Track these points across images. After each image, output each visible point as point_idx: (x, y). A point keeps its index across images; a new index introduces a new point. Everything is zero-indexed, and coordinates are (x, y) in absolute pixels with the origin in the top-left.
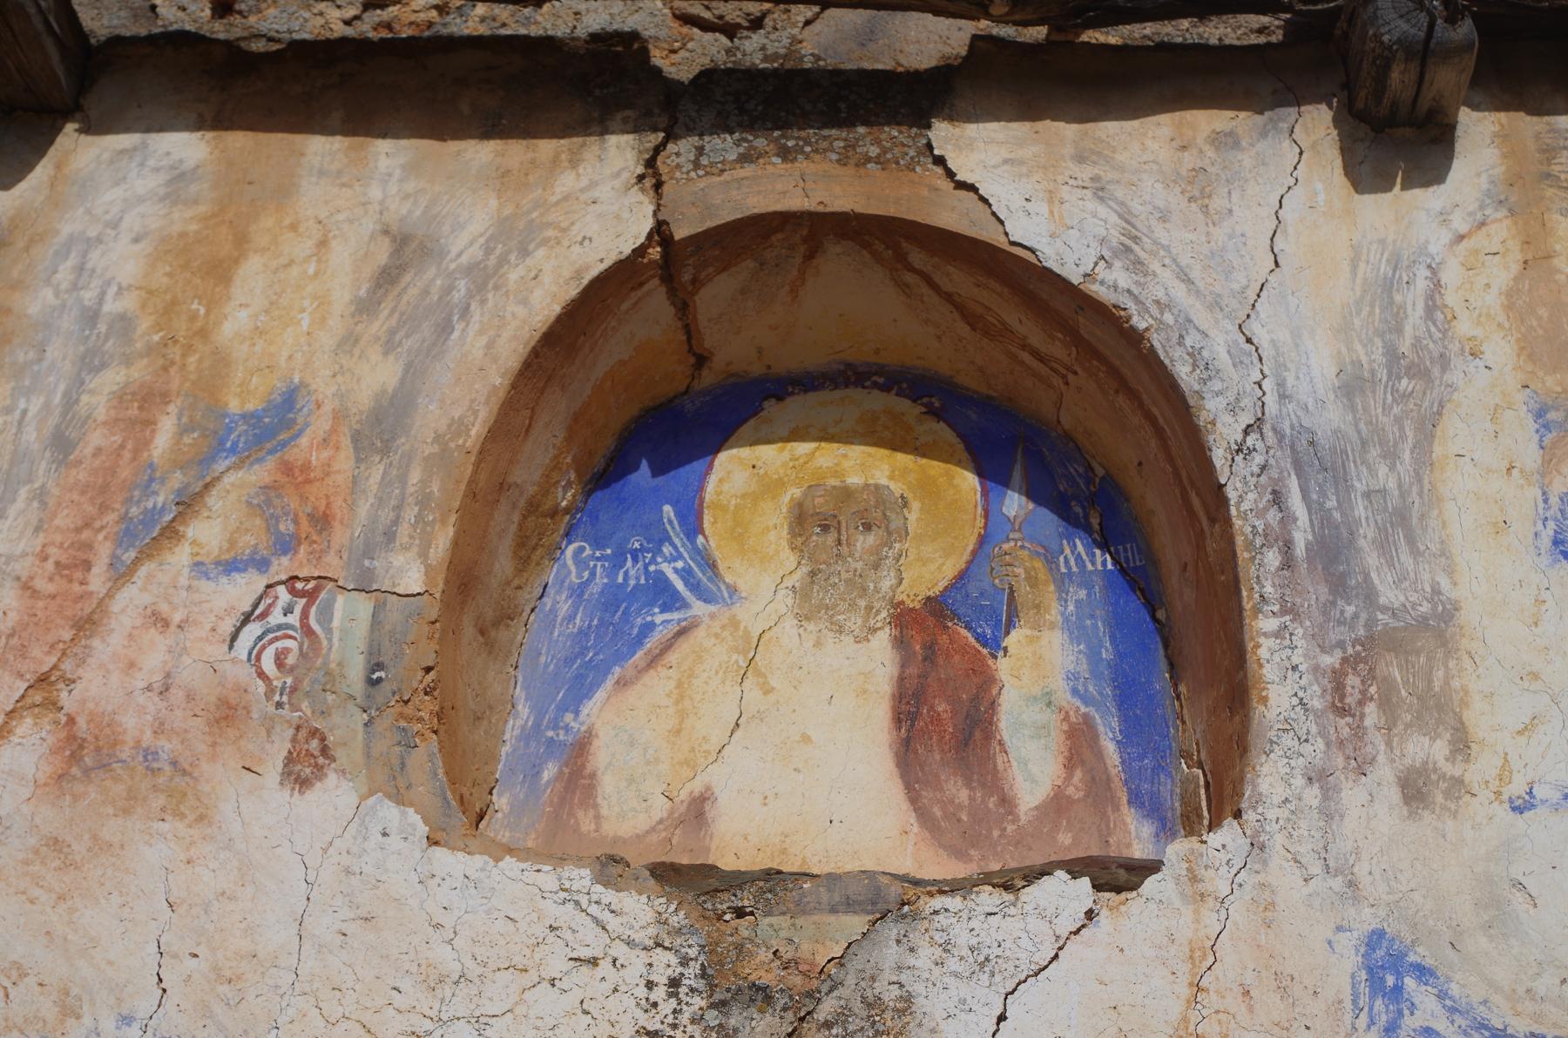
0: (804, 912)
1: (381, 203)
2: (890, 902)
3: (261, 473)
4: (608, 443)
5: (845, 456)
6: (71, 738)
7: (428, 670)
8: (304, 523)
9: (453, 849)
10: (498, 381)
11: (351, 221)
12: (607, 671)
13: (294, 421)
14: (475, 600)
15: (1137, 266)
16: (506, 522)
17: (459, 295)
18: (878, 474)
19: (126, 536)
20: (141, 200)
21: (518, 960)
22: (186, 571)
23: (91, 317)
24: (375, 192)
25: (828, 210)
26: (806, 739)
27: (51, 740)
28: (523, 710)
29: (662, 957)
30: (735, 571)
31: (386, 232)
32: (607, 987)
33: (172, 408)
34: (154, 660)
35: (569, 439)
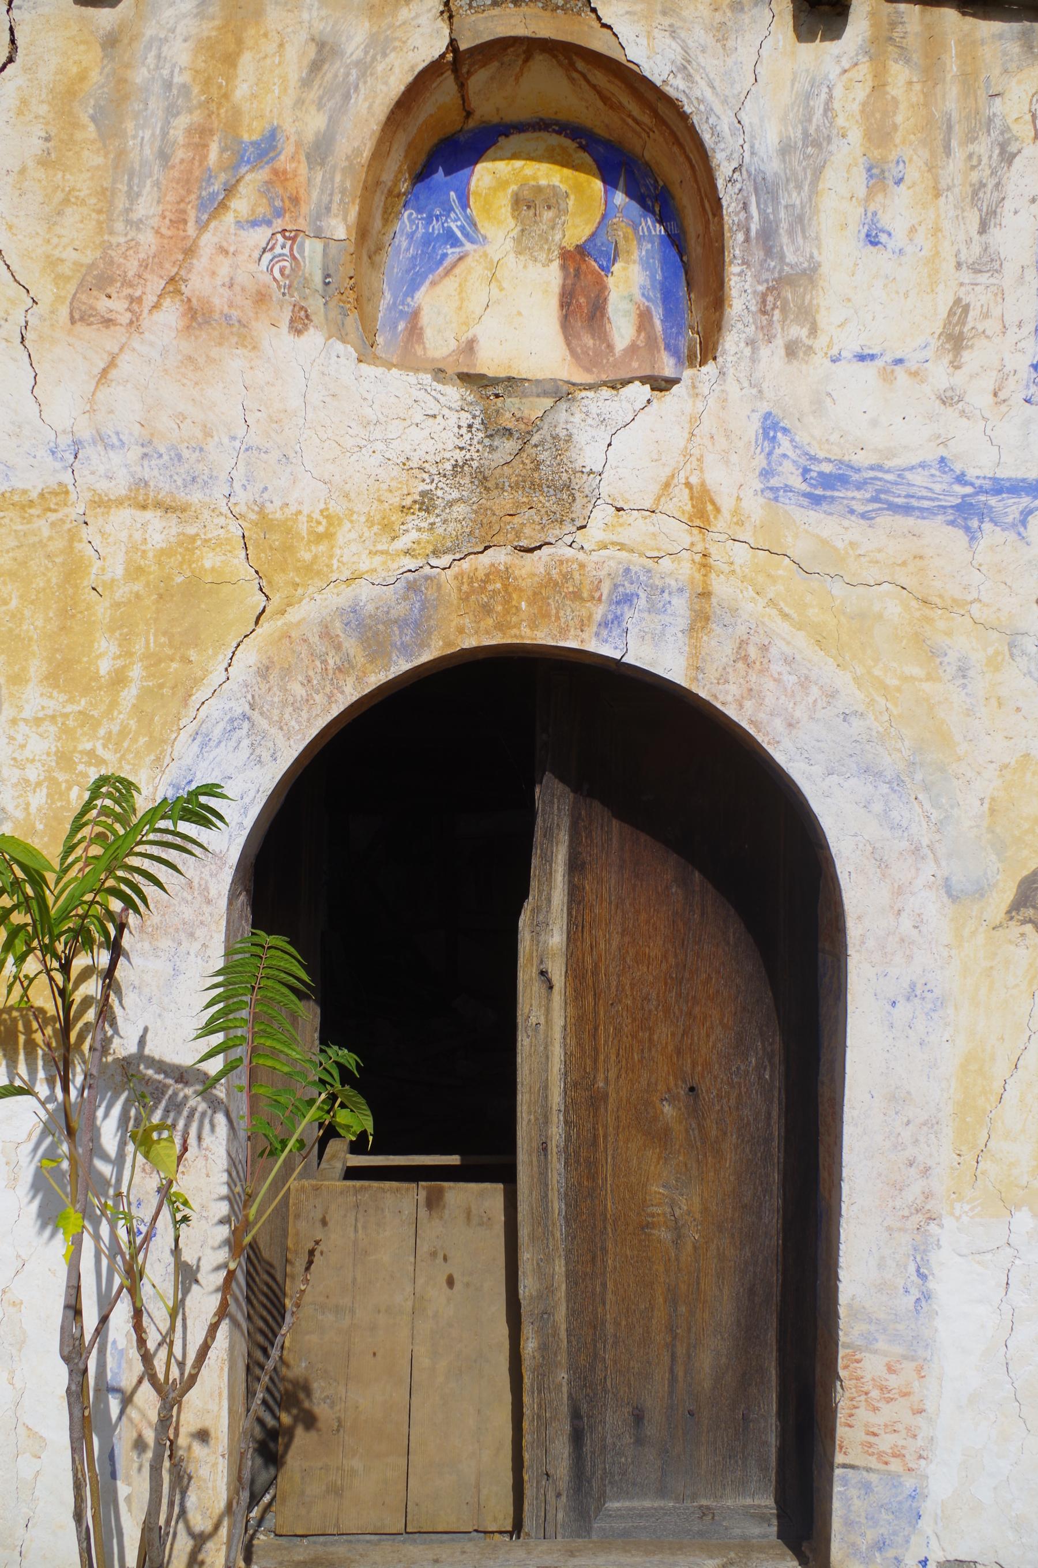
0: (525, 396)
1: (309, 22)
2: (563, 393)
3: (263, 174)
4: (423, 157)
5: (539, 169)
6: (190, 309)
7: (351, 278)
8: (287, 202)
9: (369, 364)
10: (375, 128)
11: (294, 33)
12: (426, 277)
13: (276, 146)
14: (367, 242)
15: (689, 77)
16: (379, 200)
17: (352, 78)
18: (554, 179)
19: (202, 207)
20: (185, 16)
21: (401, 415)
22: (233, 226)
23: (168, 85)
24: (305, 16)
25: (538, 36)
26: (519, 314)
27: (181, 309)
28: (388, 295)
29: (464, 415)
30: (486, 228)
31: (313, 40)
32: (441, 427)
33: (215, 138)
34: (224, 270)
35: (406, 157)
